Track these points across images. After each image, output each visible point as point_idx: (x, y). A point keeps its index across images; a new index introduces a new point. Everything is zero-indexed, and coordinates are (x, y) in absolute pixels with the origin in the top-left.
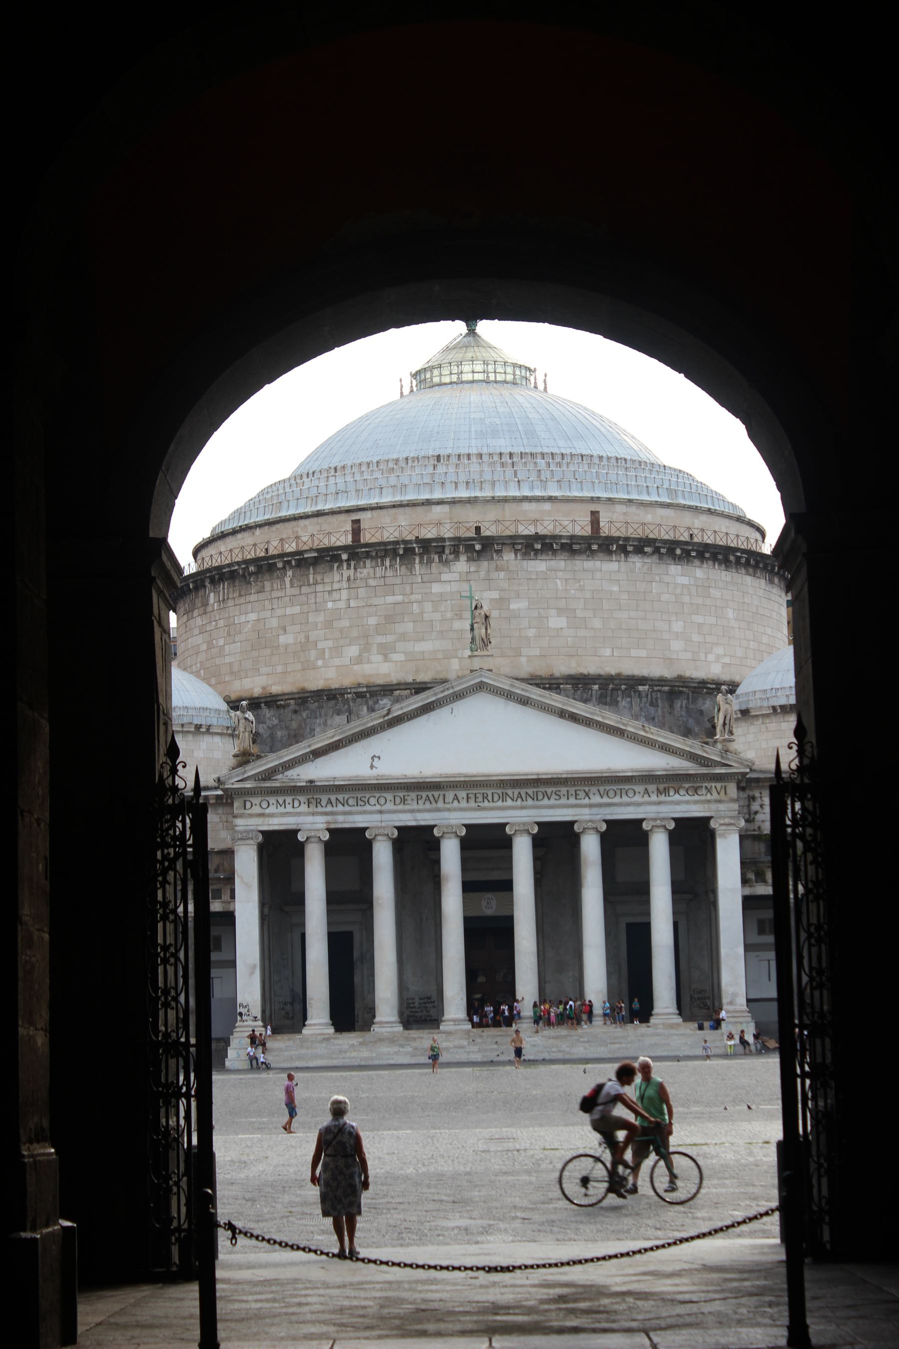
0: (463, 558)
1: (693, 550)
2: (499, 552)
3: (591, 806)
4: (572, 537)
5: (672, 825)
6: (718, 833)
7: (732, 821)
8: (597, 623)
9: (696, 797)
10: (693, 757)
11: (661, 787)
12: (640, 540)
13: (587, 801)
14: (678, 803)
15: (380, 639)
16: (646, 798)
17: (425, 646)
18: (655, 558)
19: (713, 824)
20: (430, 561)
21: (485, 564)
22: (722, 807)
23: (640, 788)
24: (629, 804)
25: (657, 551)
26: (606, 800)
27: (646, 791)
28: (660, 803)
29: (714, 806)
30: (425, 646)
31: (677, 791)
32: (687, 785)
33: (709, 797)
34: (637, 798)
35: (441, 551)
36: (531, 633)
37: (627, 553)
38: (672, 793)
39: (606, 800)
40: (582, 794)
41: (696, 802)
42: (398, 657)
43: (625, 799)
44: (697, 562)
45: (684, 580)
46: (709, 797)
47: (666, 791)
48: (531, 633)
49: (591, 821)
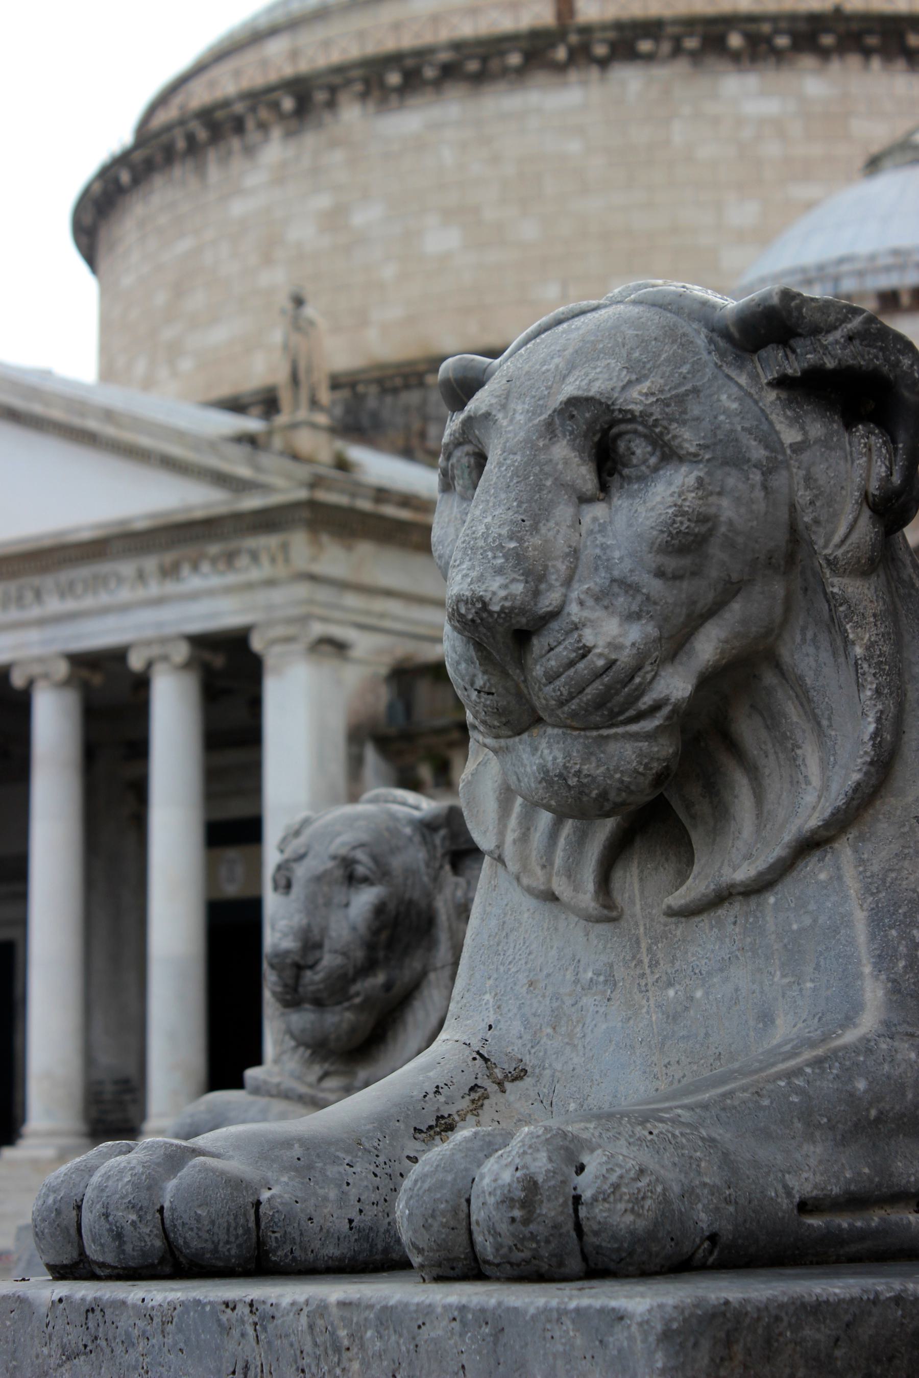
0: (276, 133)
1: (777, 32)
2: (331, 104)
3: (41, 622)
4: (458, 46)
5: (181, 652)
6: (270, 662)
7: (290, 631)
8: (529, 230)
9: (231, 579)
10: (220, 479)
11: (169, 558)
12: (619, 26)
13: (35, 612)
14: (194, 596)
15: (168, 334)
16: (141, 593)
17: (219, 335)
18: (682, 66)
19: (257, 643)
20: (229, 153)
21: (310, 140)
22: (278, 596)
23: (127, 568)
24: (104, 611)
25: (677, 51)
26: (70, 605)
27: (141, 577)
28: (159, 601)
29: (262, 597)
30: (219, 335)
31: (195, 567)
32: (214, 549)
33: (255, 574)
34: (125, 594)
35: (239, 126)
36: (389, 272)
37: (603, 63)
38: (186, 570)
39: (70, 605)
40: (29, 596)
41: (228, 590)
42: (186, 365)
43: (104, 598)
44: (808, 61)
45: (770, 107)
46: (255, 574)
47: (170, 572)
48: (389, 272)
49: (41, 660)
